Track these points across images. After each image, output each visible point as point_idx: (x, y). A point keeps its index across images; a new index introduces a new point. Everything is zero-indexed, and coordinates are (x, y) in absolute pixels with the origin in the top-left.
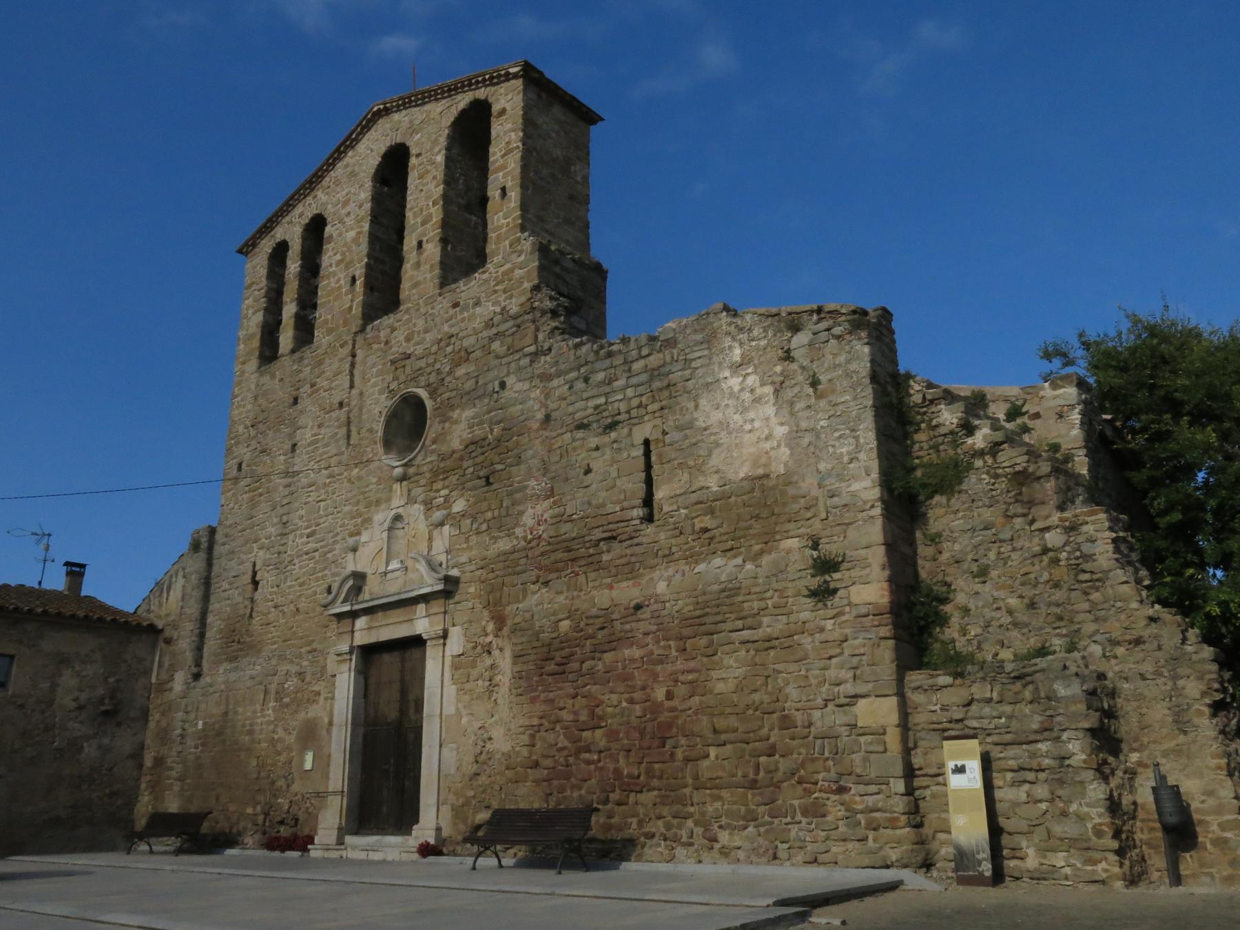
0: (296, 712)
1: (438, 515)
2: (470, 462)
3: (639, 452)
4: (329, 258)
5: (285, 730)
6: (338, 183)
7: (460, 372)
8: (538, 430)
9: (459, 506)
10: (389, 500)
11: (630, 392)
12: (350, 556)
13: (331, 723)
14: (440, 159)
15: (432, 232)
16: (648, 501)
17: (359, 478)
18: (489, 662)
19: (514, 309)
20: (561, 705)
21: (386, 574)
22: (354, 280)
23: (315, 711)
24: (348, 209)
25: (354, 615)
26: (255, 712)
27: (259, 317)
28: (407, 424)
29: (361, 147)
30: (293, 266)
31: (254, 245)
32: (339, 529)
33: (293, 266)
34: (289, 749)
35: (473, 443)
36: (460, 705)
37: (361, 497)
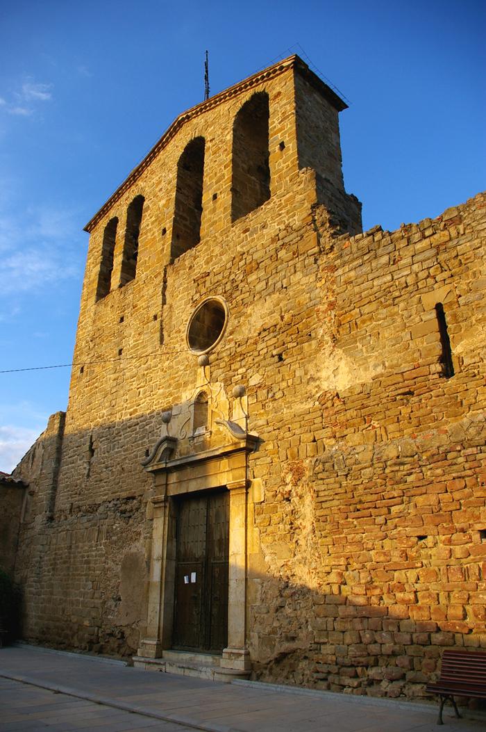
0: (122, 547)
1: (236, 389)
2: (264, 345)
3: (434, 314)
4: (147, 222)
5: (114, 561)
6: (153, 172)
7: (252, 278)
8: (325, 312)
9: (255, 380)
10: (195, 381)
11: (415, 267)
12: (164, 426)
13: (150, 557)
14: (229, 137)
15: (226, 184)
16: (446, 358)
17: (170, 368)
18: (289, 508)
19: (296, 222)
20: (370, 546)
21: (193, 438)
22: (164, 231)
23: (138, 547)
24: (160, 187)
25: (167, 471)
26: (91, 547)
27: (98, 268)
28: (208, 326)
29: (169, 147)
30: (121, 231)
31: (96, 223)
33: (121, 231)
34: (116, 576)
35: (265, 330)
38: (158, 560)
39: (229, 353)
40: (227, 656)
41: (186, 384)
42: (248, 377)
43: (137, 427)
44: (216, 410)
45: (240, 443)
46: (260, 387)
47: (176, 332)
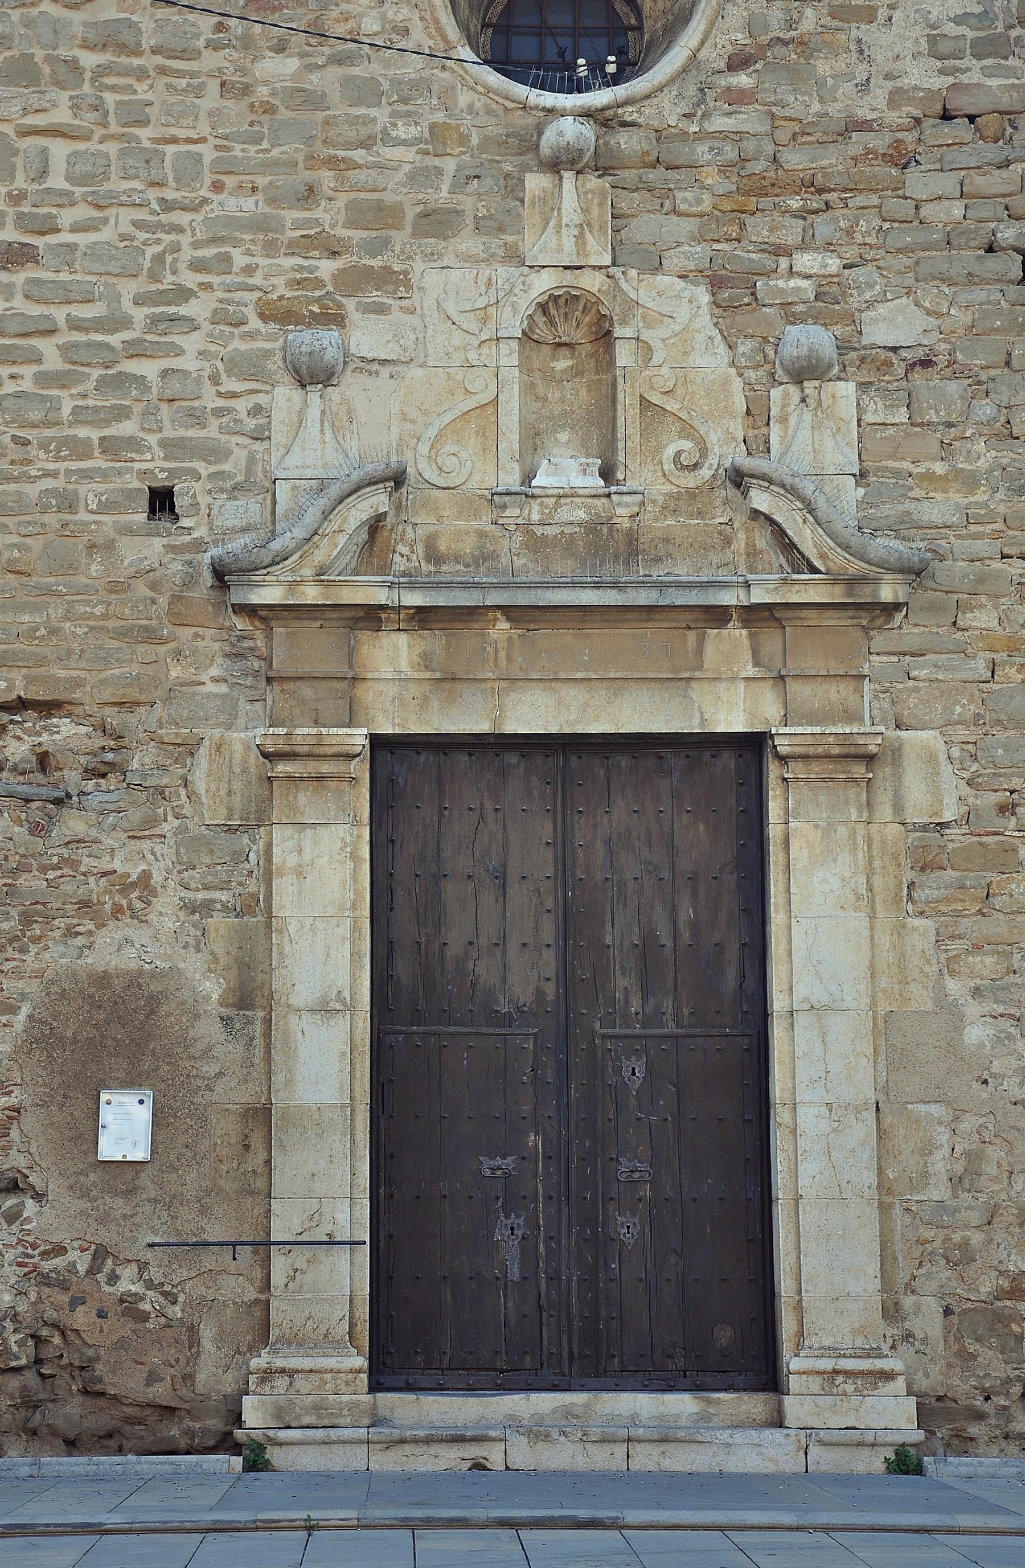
2: (949, 183)
9: (894, 324)
32: (191, 279)
35: (946, 116)
36: (952, 985)
37: (327, 178)
38: (324, 1010)
39: (730, 153)
40: (815, 1384)
41: (436, 223)
42: (855, 301)
43: (46, 346)
44: (672, 406)
45: (876, 581)
46: (926, 363)
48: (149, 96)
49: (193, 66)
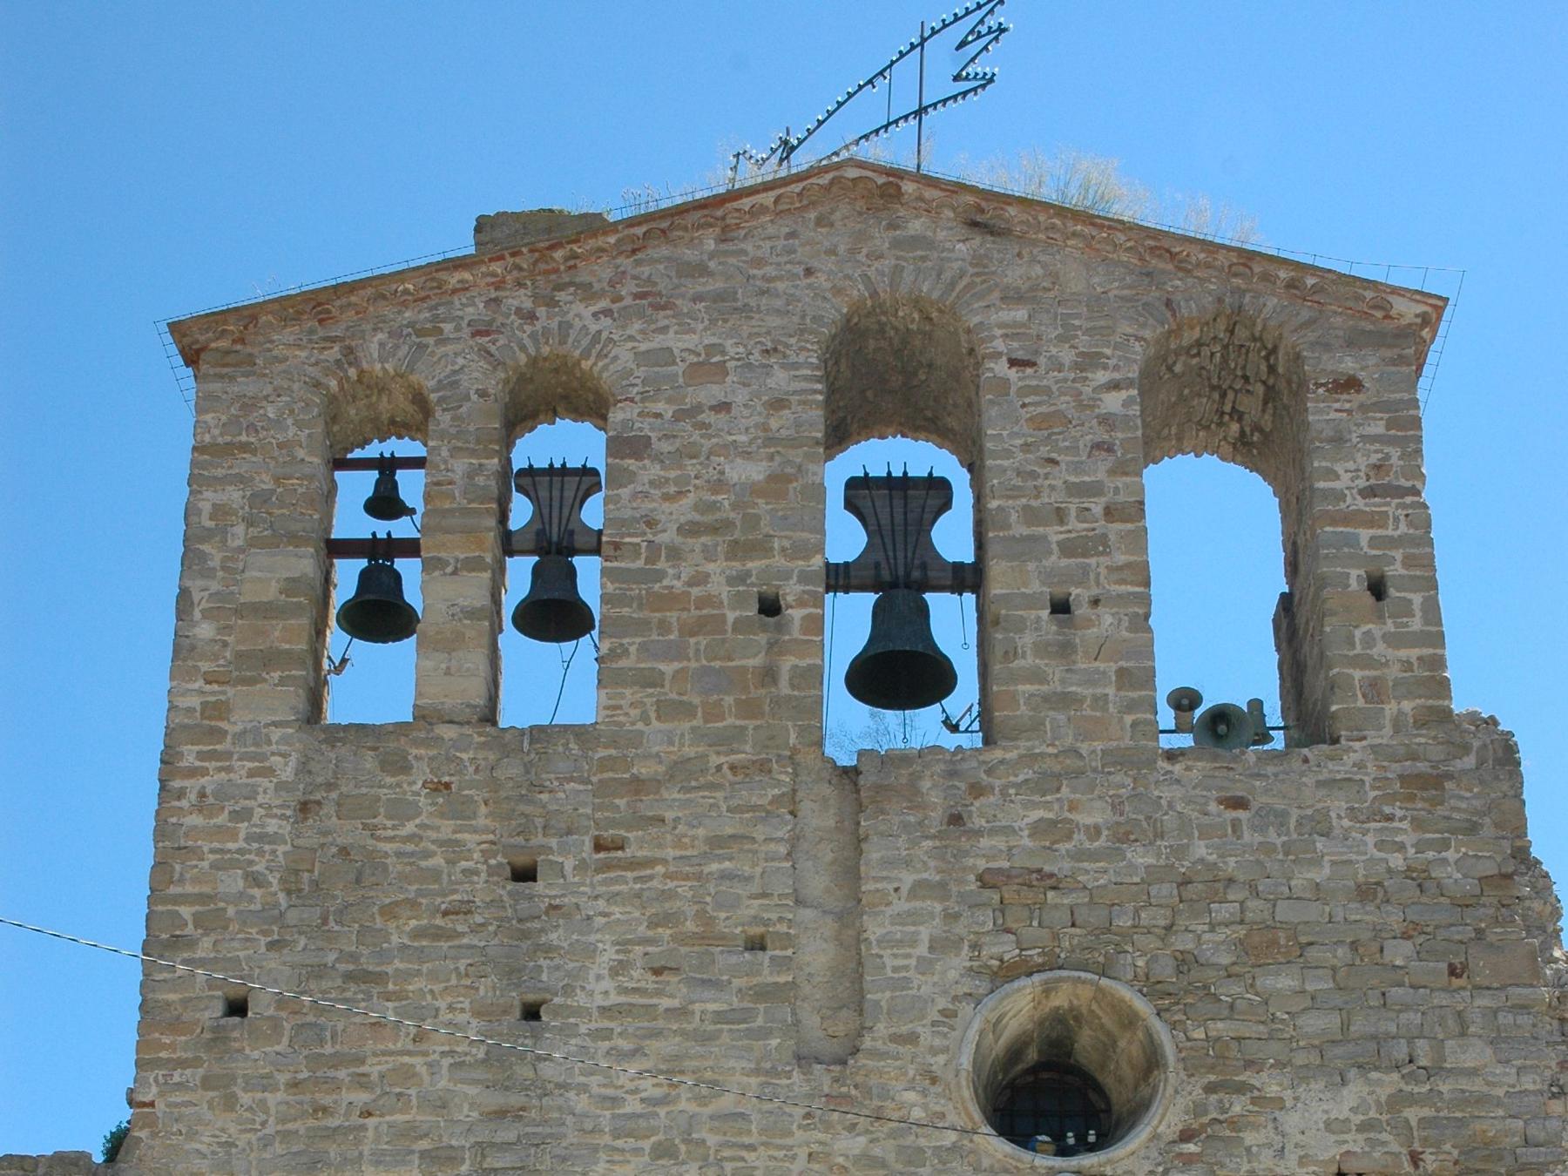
47: (896, 1038)
48: (756, 1164)
49: (789, 1141)
